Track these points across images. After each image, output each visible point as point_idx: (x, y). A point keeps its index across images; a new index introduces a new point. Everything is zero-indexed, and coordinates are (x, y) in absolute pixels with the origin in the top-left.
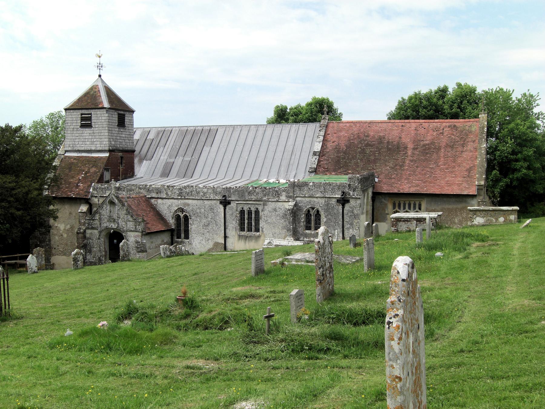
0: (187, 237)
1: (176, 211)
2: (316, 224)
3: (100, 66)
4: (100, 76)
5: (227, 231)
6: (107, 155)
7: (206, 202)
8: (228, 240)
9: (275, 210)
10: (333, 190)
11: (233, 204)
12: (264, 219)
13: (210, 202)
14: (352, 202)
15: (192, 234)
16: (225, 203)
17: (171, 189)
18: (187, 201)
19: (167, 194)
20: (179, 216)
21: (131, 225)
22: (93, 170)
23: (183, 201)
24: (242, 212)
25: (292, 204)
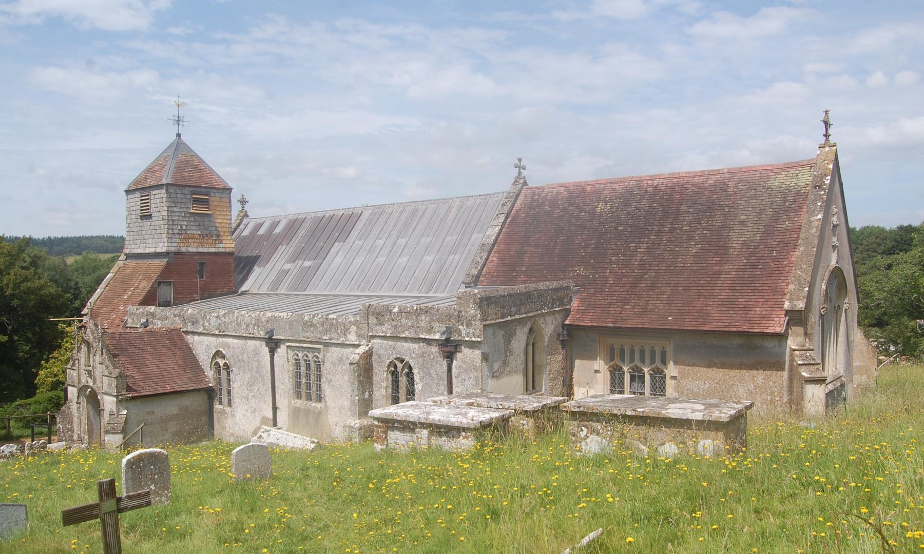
0: (230, 405)
1: (214, 357)
3: (179, 121)
4: (179, 135)
5: (277, 396)
7: (250, 342)
8: (279, 413)
11: (282, 351)
12: (327, 378)
15: (236, 400)
16: (273, 344)
17: (208, 317)
19: (204, 326)
20: (217, 363)
22: (144, 283)
23: (221, 340)
24: (298, 364)
25: (361, 350)
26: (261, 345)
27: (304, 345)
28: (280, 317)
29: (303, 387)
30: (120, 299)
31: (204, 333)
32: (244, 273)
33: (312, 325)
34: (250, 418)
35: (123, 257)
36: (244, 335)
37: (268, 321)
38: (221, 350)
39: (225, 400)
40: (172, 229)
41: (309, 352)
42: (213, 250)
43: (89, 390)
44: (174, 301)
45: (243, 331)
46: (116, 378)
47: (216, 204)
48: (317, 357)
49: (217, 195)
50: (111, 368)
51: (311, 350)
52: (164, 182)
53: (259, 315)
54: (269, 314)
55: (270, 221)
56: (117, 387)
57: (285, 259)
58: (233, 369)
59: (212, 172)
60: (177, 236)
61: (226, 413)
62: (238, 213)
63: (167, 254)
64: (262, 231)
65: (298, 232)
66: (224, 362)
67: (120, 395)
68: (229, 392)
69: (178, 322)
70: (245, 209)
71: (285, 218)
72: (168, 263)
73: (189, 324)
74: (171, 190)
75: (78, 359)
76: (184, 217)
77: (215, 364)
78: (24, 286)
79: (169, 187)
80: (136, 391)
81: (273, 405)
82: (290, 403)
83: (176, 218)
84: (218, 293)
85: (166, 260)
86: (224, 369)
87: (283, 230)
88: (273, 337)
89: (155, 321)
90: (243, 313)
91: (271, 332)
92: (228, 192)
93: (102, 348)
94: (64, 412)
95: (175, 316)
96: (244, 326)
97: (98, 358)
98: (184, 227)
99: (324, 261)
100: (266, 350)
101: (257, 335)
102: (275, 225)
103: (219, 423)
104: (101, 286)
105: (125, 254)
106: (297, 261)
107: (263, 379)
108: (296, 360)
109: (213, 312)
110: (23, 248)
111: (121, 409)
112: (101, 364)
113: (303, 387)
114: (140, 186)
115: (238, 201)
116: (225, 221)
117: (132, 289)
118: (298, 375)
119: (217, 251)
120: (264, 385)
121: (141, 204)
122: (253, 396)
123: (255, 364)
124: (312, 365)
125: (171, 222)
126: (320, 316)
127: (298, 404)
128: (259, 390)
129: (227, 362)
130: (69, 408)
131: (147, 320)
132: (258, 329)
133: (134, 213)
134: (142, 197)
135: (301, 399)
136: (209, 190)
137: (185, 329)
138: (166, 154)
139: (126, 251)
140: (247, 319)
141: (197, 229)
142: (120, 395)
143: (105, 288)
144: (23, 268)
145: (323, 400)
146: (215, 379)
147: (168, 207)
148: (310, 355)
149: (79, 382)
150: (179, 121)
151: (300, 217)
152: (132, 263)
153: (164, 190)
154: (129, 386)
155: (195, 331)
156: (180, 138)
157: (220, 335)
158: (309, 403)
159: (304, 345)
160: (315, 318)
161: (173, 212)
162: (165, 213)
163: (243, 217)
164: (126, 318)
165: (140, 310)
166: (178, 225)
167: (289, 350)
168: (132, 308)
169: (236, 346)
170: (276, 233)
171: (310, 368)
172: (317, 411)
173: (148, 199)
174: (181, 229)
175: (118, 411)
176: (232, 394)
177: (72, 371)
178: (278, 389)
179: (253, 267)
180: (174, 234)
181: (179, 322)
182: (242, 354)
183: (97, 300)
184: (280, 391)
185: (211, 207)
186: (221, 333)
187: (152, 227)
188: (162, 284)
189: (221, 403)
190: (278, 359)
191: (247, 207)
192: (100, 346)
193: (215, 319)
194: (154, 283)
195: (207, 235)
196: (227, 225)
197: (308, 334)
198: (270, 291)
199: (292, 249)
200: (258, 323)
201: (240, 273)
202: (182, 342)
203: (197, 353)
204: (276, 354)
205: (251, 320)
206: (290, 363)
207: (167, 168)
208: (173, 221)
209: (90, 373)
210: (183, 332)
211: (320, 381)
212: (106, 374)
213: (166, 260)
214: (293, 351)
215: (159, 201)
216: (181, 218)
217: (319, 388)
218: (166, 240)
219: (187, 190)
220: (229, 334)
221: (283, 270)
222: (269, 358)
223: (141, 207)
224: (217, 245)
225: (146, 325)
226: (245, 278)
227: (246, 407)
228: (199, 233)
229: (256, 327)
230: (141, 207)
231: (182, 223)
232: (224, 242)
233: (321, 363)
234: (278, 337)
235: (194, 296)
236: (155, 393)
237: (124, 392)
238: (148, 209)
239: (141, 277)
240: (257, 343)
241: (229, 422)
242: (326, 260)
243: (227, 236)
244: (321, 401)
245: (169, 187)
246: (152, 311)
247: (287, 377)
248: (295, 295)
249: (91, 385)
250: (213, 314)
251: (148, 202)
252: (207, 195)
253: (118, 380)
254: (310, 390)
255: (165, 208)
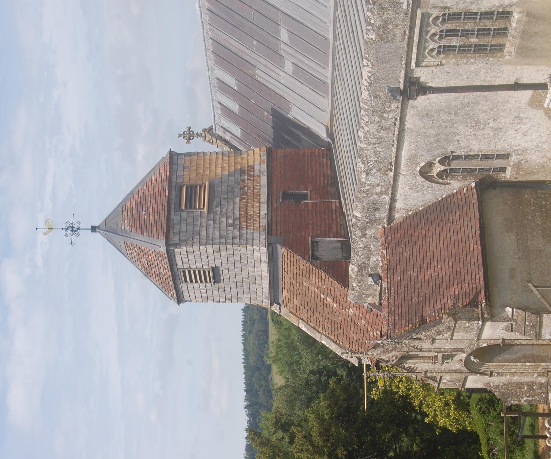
1: (429, 179)
4: (94, 229)
5: (498, 82)
7: (409, 123)
15: (500, 146)
17: (368, 187)
19: (381, 193)
22: (314, 279)
23: (403, 168)
26: (414, 107)
27: (416, 39)
28: (369, 77)
29: (484, 40)
30: (337, 314)
31: (392, 194)
32: (300, 133)
33: (384, 27)
34: (529, 125)
35: (275, 308)
36: (396, 133)
37: (376, 97)
38: (418, 169)
39: (498, 163)
40: (234, 238)
41: (428, 32)
42: (264, 180)
43: (472, 358)
44: (341, 237)
45: (391, 135)
46: (456, 321)
47: (193, 175)
48: (437, 18)
49: (180, 173)
50: (440, 327)
51: (424, 29)
52: (163, 249)
53: (365, 110)
54: (365, 95)
55: (218, 94)
56: (469, 320)
57: (278, 71)
58: (450, 149)
59: (146, 181)
60: (244, 231)
61: (519, 163)
62: (206, 143)
63: (270, 246)
64: (235, 107)
65: (234, 50)
66: (438, 164)
67: (483, 315)
68: (486, 157)
69: (376, 231)
70: (200, 131)
71: (213, 70)
72: (285, 244)
73: (377, 215)
74: (175, 239)
75: (426, 372)
76: (214, 221)
77: (441, 177)
78: (318, 441)
79: (171, 242)
80: (477, 294)
81: (511, 89)
82: (509, 63)
83: (217, 233)
84: (329, 172)
85: (279, 247)
86: (449, 165)
87: (232, 74)
88: (402, 88)
89: (371, 265)
90: (361, 134)
91: (394, 92)
92: (175, 157)
93: (411, 339)
94: (503, 394)
95: (364, 235)
96: (383, 133)
97: (426, 345)
98: (230, 221)
99: (281, 8)
100: (422, 101)
101: (397, 114)
102: (223, 87)
103: (534, 174)
104: (318, 339)
105: (271, 304)
106: (281, 52)
107: (468, 105)
108: (439, 52)
109: (360, 179)
110: (264, 440)
111: (504, 315)
112: (434, 341)
113: (484, 40)
114: (171, 283)
115: (188, 142)
116: (220, 161)
117: (322, 296)
118: (464, 49)
119: (265, 174)
120: (477, 103)
121: (196, 281)
122: (495, 120)
123: (444, 117)
124: (449, 26)
125: (223, 240)
126: (369, 14)
127: (512, 49)
128: (485, 112)
129: (438, 159)
130: (497, 387)
131: (370, 275)
132: (388, 112)
133: (210, 292)
134: (186, 281)
135: (504, 45)
136: (174, 185)
137: (385, 221)
138: (123, 246)
139: (266, 303)
140: (372, 128)
141: (232, 202)
142: (483, 315)
143: (321, 334)
144: (292, 441)
145: (508, 9)
146: (464, 178)
147: (200, 244)
148: (433, 29)
149: (460, 371)
150: (73, 229)
151: (211, 48)
152: (283, 296)
153: (177, 250)
154: (470, 303)
155: (388, 206)
156: (98, 227)
157: (396, 170)
158: (511, 32)
159: (416, 39)
160: (372, 21)
161: (207, 237)
162: (210, 249)
163: (212, 135)
164: (366, 305)
165: (355, 285)
166: (227, 230)
167: (424, 64)
168: (352, 296)
169: (413, 146)
170: (237, 85)
171: (453, 30)
172: (525, 19)
173: (189, 272)
174: (233, 225)
175: (506, 319)
176: (490, 153)
177: (444, 381)
178: (485, 81)
179: (289, 120)
180: (240, 236)
181: (373, 230)
182: (427, 136)
183: (339, 345)
184: (489, 79)
185: (199, 182)
186: (393, 168)
187: (231, 267)
188: (316, 254)
189: (503, 170)
190: (437, 80)
191: (198, 129)
192: (407, 342)
193: (370, 177)
194: (314, 265)
195: (241, 189)
196: (226, 158)
197: (399, 34)
198: (327, 94)
199: (262, 60)
200: (379, 112)
201: (299, 140)
202: (405, 225)
203: (423, 203)
204: (428, 85)
205: (373, 122)
206: (444, 62)
207: (143, 245)
208: (221, 237)
209: (448, 357)
210: (389, 224)
211: (476, 14)
212: (449, 334)
213: (279, 247)
214: (425, 57)
215: (191, 257)
216: (217, 226)
217: (487, 15)
218: (249, 248)
219: (175, 217)
220: (394, 156)
221: (294, 73)
222: (433, 97)
223: (201, 281)
224: (257, 173)
225: (377, 278)
226: (307, 132)
227: (511, 132)
228: (238, 200)
229: (385, 115)
230: (201, 281)
231: (224, 224)
232: (251, 163)
233: (447, 11)
234: (402, 80)
235: (334, 208)
236: (481, 267)
237: (479, 311)
238: (204, 272)
239: (304, 284)
240: (410, 113)
241: (534, 158)
242: (278, 5)
243: (242, 159)
244: (509, 13)
245: (171, 242)
246: (356, 269)
247: (467, 66)
248: (334, 55)
249: (464, 355)
250: (363, 180)
251: (194, 272)
252: (181, 188)
253: (460, 318)
254: (489, 30)
255: (203, 248)
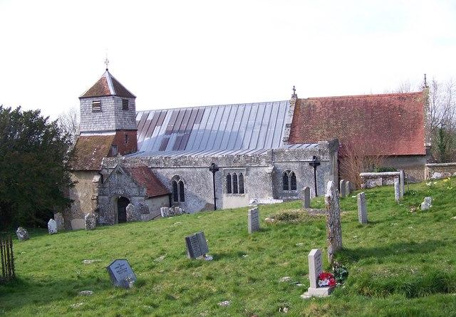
0: (183, 200)
2: (292, 184)
4: (107, 70)
6: (115, 134)
7: (198, 170)
9: (257, 174)
10: (306, 156)
13: (201, 170)
14: (323, 165)
16: (214, 169)
18: (181, 169)
20: (175, 183)
21: (135, 191)
23: (179, 170)
